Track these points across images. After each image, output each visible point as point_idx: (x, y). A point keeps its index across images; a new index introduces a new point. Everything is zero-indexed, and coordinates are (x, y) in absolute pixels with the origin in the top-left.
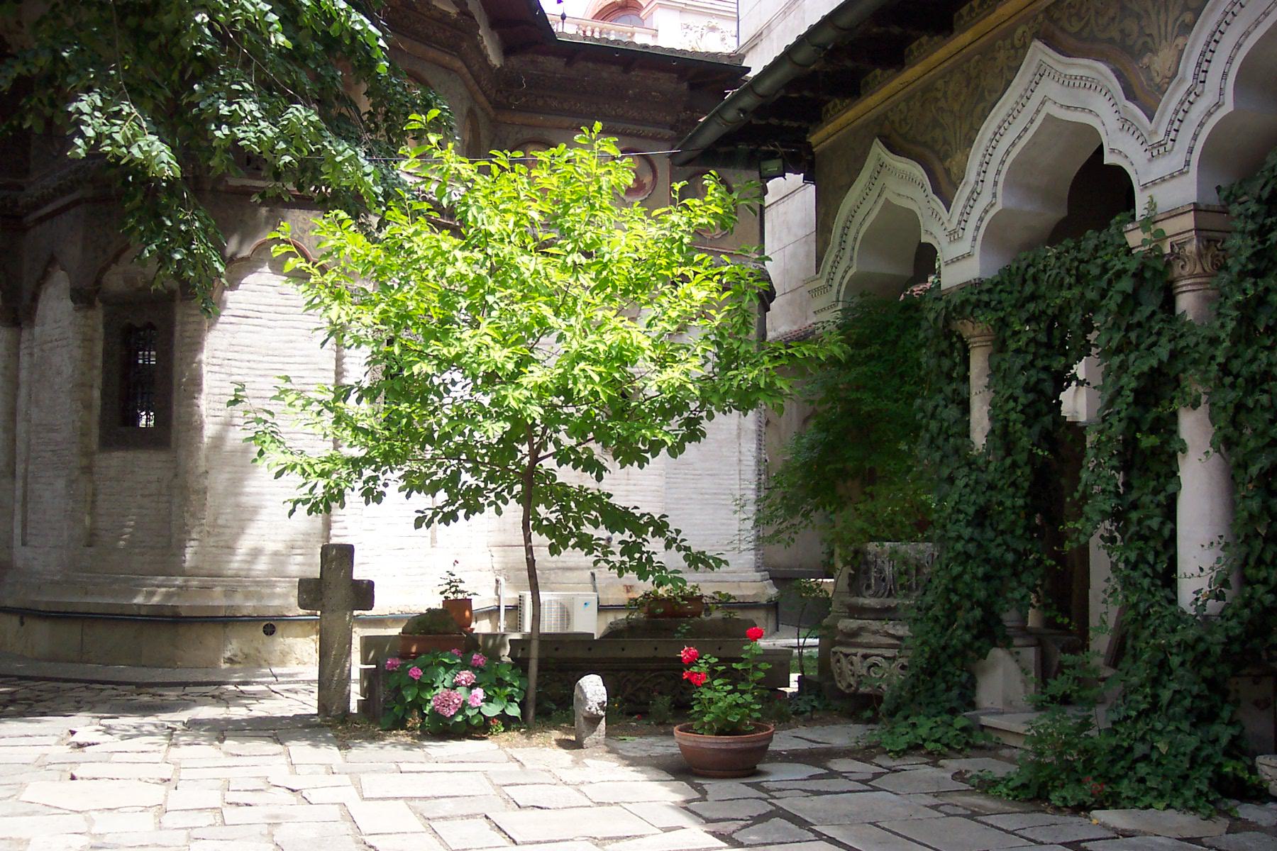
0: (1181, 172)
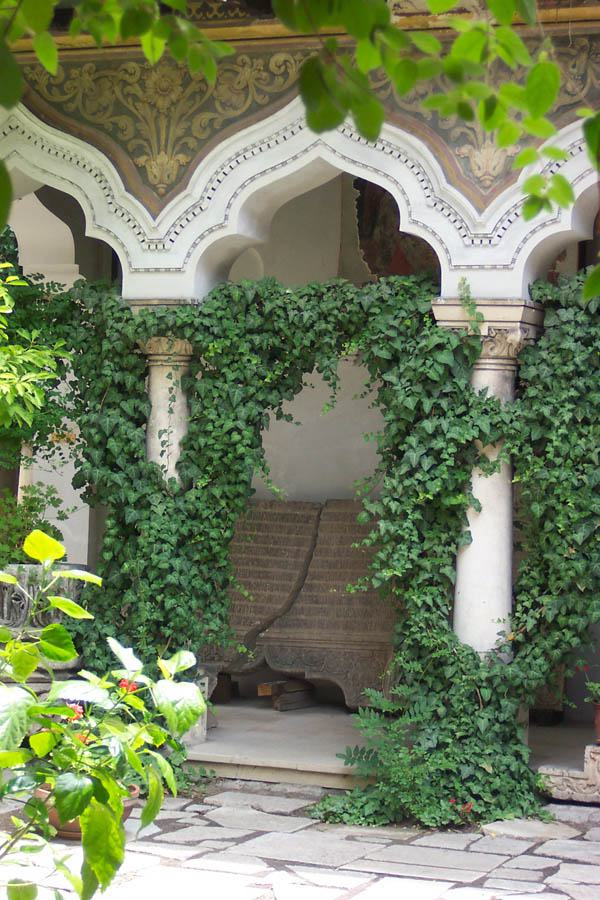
0: (506, 267)
